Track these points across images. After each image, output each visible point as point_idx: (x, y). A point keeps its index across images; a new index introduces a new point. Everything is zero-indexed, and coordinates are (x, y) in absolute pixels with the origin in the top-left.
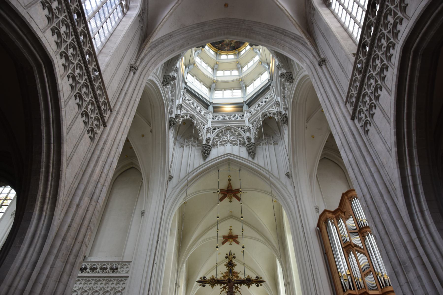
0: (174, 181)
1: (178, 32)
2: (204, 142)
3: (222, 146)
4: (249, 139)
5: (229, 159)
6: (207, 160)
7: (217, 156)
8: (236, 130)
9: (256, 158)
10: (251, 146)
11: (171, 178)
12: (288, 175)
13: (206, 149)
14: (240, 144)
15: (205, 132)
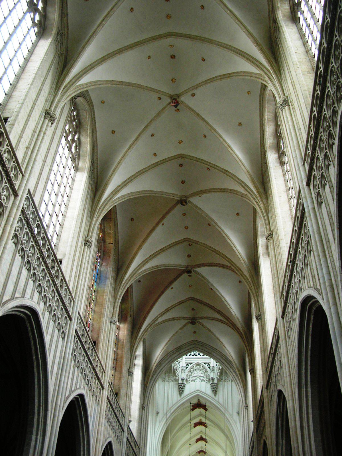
0: (160, 415)
1: (164, 359)
2: (180, 381)
3: (193, 381)
4: (213, 379)
5: (198, 395)
6: (183, 396)
7: (189, 393)
8: (204, 367)
9: (217, 395)
10: (214, 386)
11: (158, 413)
12: (238, 413)
13: (181, 387)
14: (206, 380)
15: (180, 369)
